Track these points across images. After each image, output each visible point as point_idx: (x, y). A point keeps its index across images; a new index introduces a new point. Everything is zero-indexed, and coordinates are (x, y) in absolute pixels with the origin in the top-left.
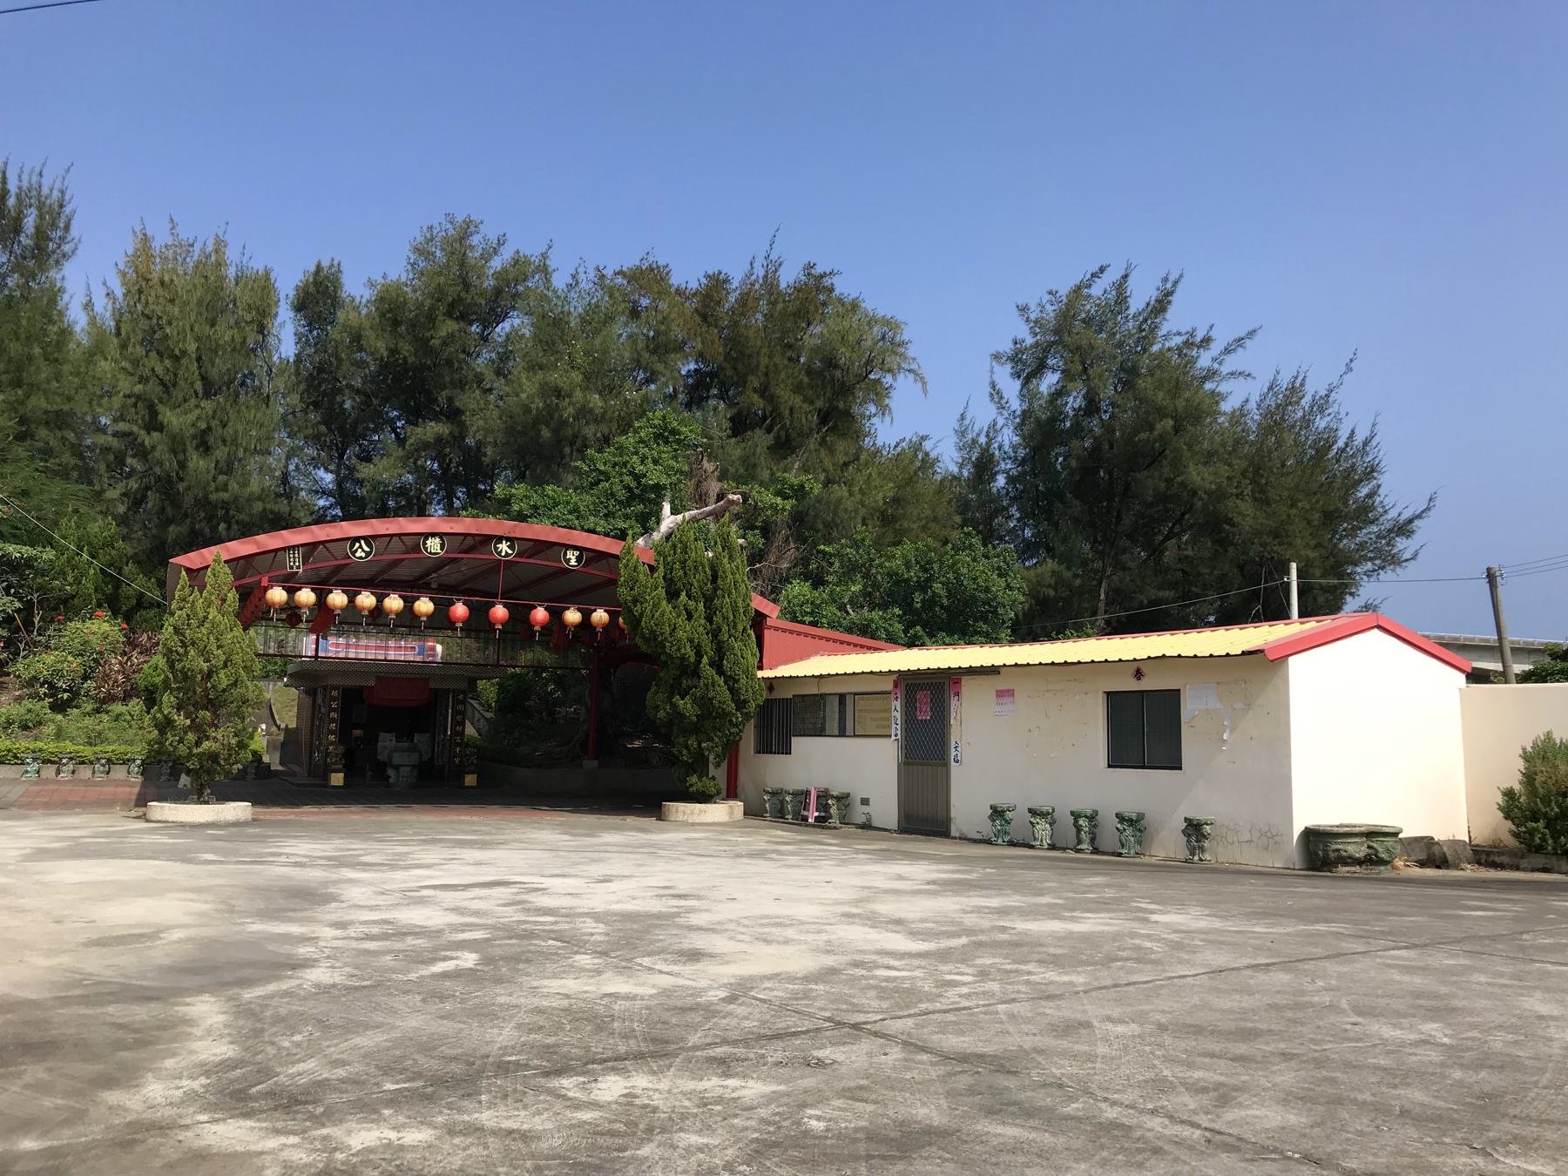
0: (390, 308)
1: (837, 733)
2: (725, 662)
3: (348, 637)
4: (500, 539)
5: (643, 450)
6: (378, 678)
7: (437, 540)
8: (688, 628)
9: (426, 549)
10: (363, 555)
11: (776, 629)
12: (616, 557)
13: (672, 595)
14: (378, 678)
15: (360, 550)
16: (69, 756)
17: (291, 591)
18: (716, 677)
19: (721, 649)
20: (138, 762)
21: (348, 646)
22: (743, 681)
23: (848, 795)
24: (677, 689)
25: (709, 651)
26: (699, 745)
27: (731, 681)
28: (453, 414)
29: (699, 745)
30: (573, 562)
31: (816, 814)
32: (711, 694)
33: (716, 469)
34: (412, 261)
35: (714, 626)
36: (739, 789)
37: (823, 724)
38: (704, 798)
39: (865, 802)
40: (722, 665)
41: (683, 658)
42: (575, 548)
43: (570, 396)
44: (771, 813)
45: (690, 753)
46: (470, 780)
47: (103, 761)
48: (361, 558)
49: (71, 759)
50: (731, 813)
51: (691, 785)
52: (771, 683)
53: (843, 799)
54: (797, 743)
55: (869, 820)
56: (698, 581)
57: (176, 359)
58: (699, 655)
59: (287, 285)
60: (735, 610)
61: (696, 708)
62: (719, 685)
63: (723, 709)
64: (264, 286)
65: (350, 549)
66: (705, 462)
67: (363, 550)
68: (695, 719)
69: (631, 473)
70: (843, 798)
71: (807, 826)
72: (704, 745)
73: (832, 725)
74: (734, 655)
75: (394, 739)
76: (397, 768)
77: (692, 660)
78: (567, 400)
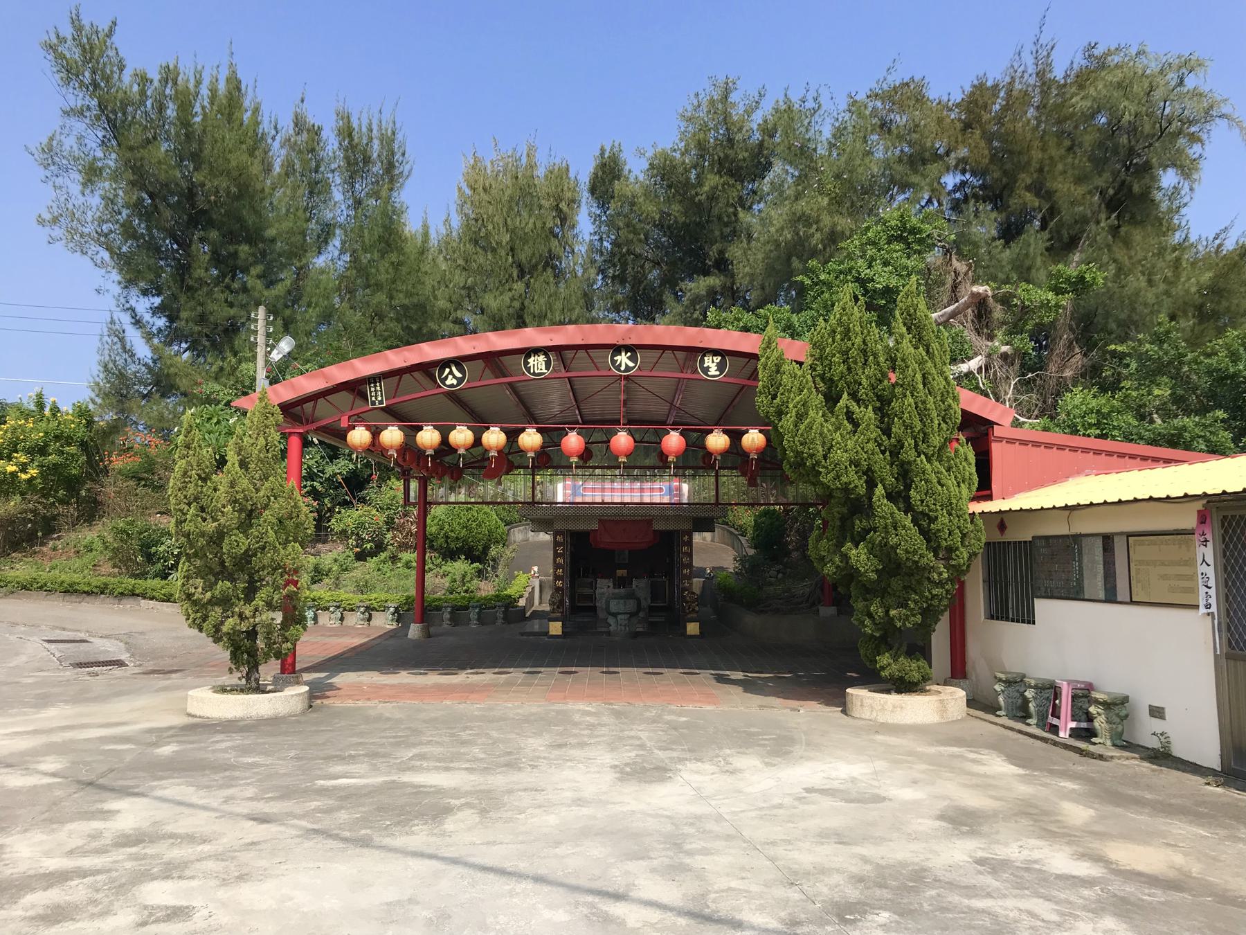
0: (664, 171)
1: (1102, 596)
2: (912, 493)
3: (603, 481)
4: (617, 349)
5: (871, 251)
6: (602, 522)
7: (542, 358)
8: (850, 444)
9: (528, 369)
10: (455, 382)
11: (1011, 441)
12: (755, 357)
13: (831, 399)
14: (602, 522)
15: (450, 377)
16: (335, 604)
17: (412, 430)
18: (900, 515)
19: (905, 474)
20: (392, 610)
21: (642, 490)
22: (943, 519)
23: (1125, 700)
24: (846, 532)
25: (886, 473)
26: (887, 612)
27: (924, 522)
28: (722, 265)
29: (887, 612)
30: (713, 371)
31: (1073, 725)
32: (893, 540)
33: (970, 269)
34: (683, 129)
35: (893, 440)
36: (969, 667)
37: (1080, 581)
38: (904, 686)
39: (1157, 712)
40: (909, 497)
41: (846, 489)
42: (715, 352)
43: (817, 222)
44: (1007, 710)
45: (875, 624)
46: (693, 628)
47: (362, 609)
48: (452, 386)
49: (338, 607)
50: (943, 710)
51: (883, 668)
52: (1002, 520)
53: (1118, 706)
54: (1042, 607)
55: (1166, 745)
56: (868, 377)
57: (494, 250)
58: (871, 485)
59: (583, 171)
60: (923, 414)
61: (876, 561)
62: (904, 527)
63: (916, 562)
64: (560, 175)
65: (439, 377)
66: (954, 261)
67: (454, 377)
68: (874, 576)
69: (857, 280)
70: (1115, 704)
71: (1055, 744)
72: (893, 613)
73: (1095, 582)
74: (927, 481)
75: (611, 585)
76: (615, 615)
77: (862, 490)
78: (815, 226)
